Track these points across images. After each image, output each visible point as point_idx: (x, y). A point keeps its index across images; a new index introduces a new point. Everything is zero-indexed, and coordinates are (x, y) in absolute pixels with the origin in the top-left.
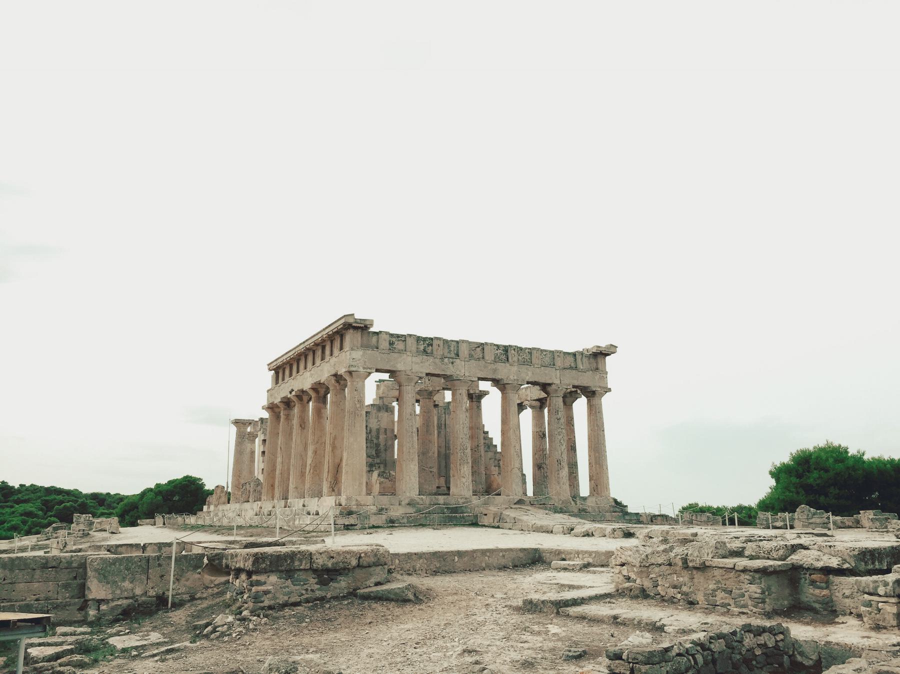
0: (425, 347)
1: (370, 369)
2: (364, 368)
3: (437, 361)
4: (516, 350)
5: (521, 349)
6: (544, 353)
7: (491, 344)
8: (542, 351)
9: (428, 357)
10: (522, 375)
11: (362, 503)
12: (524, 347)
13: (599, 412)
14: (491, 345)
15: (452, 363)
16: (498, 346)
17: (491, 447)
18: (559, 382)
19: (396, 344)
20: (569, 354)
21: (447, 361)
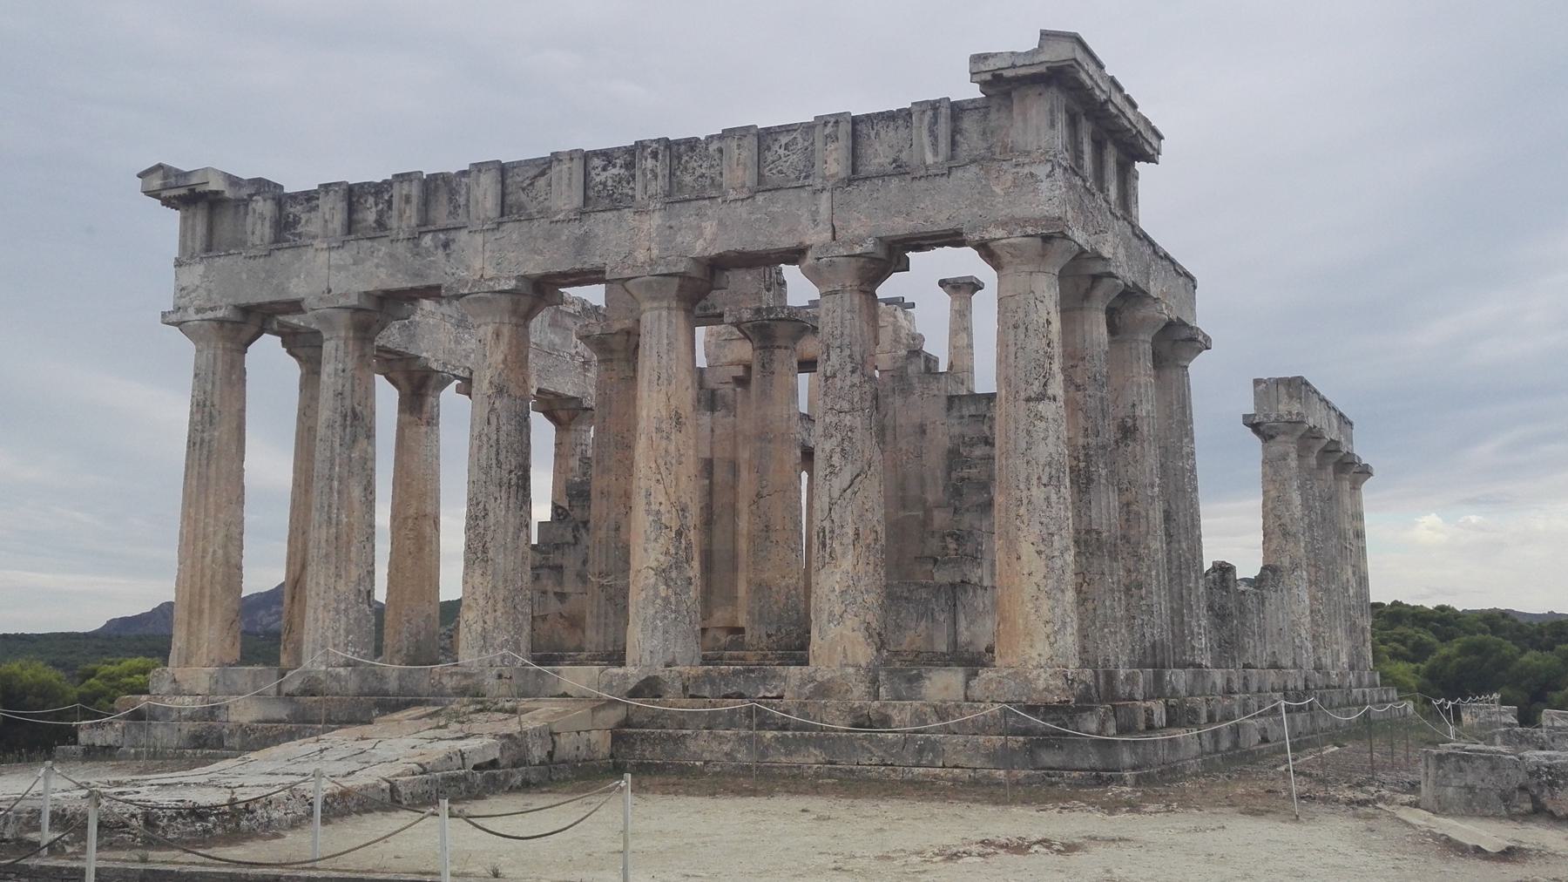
0: (380, 214)
1: (212, 309)
2: (198, 311)
3: (401, 248)
4: (660, 156)
5: (692, 144)
6: (784, 140)
7: (571, 155)
8: (765, 137)
9: (375, 244)
10: (679, 239)
11: (186, 687)
12: (702, 130)
13: (1015, 327)
14: (571, 159)
15: (446, 245)
16: (607, 156)
17: (965, 491)
18: (829, 235)
19: (303, 221)
20: (890, 117)
21: (429, 243)
